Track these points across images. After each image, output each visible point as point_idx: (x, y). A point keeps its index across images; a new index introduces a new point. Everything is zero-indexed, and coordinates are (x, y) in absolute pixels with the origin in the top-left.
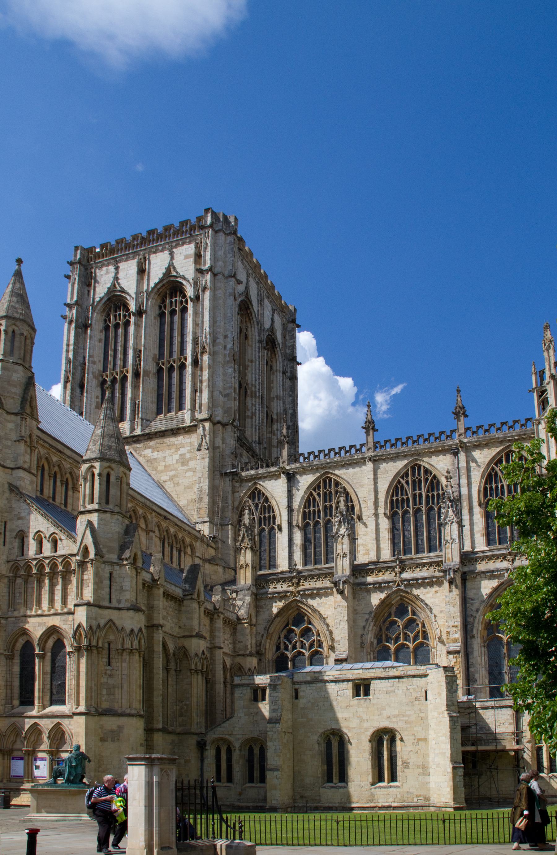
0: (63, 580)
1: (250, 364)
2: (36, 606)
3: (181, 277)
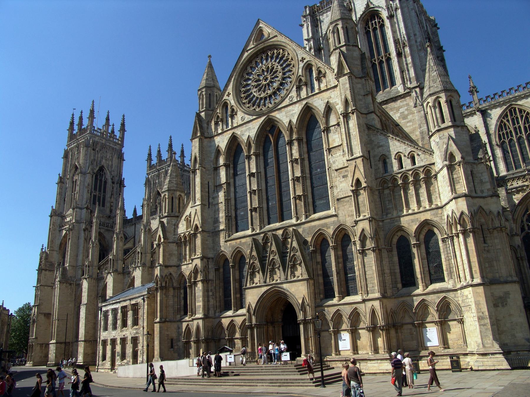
0: (426, 185)
2: (406, 207)
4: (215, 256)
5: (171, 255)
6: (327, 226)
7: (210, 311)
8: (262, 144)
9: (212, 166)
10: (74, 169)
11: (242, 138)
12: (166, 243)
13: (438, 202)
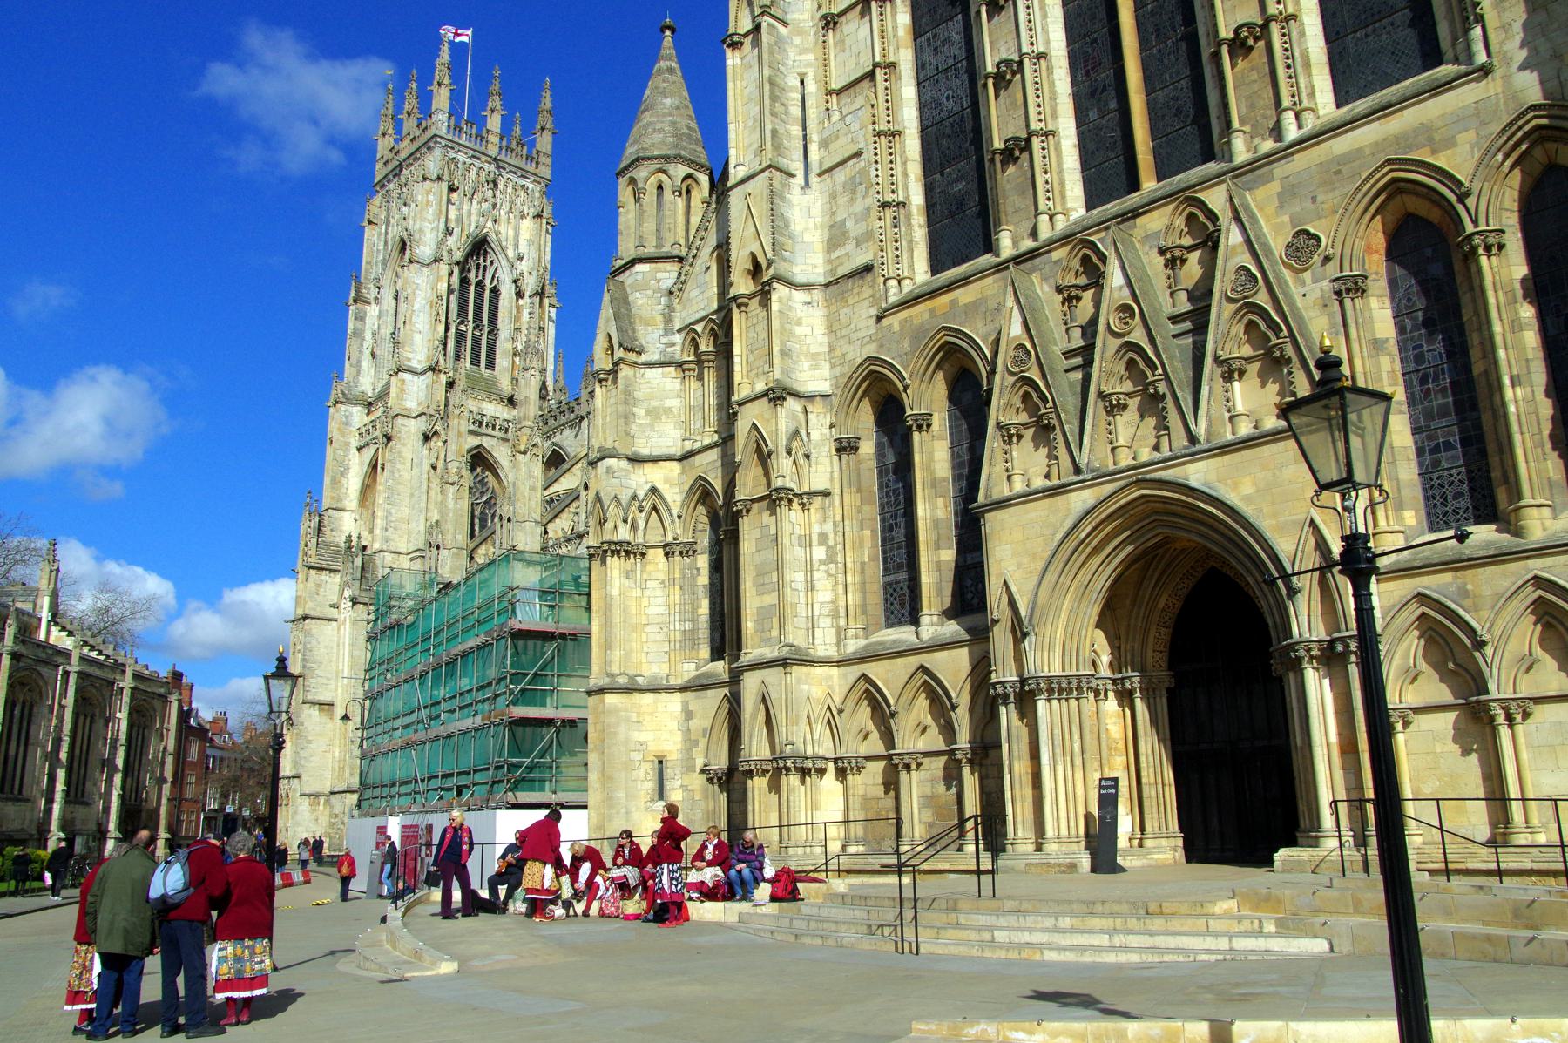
4: (837, 387)
5: (654, 414)
6: (1431, 140)
7: (818, 633)
9: (818, 15)
10: (395, 255)
12: (634, 364)
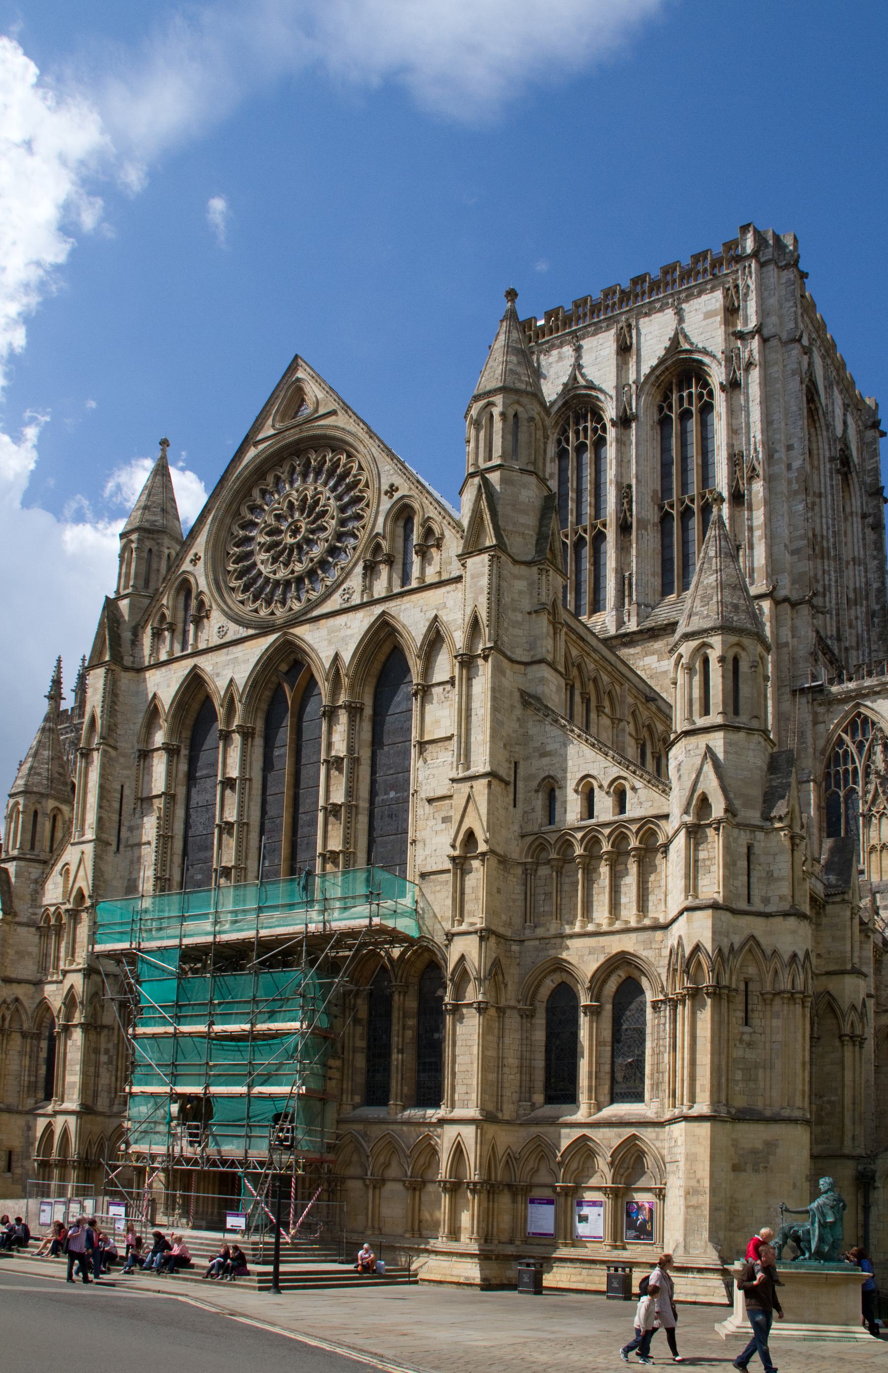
0: (639, 866)
1: (817, 500)
3: (699, 352)
7: (99, 1099)
8: (264, 706)
9: (137, 747)
11: (214, 682)
12: (8, 923)
13: (658, 912)
